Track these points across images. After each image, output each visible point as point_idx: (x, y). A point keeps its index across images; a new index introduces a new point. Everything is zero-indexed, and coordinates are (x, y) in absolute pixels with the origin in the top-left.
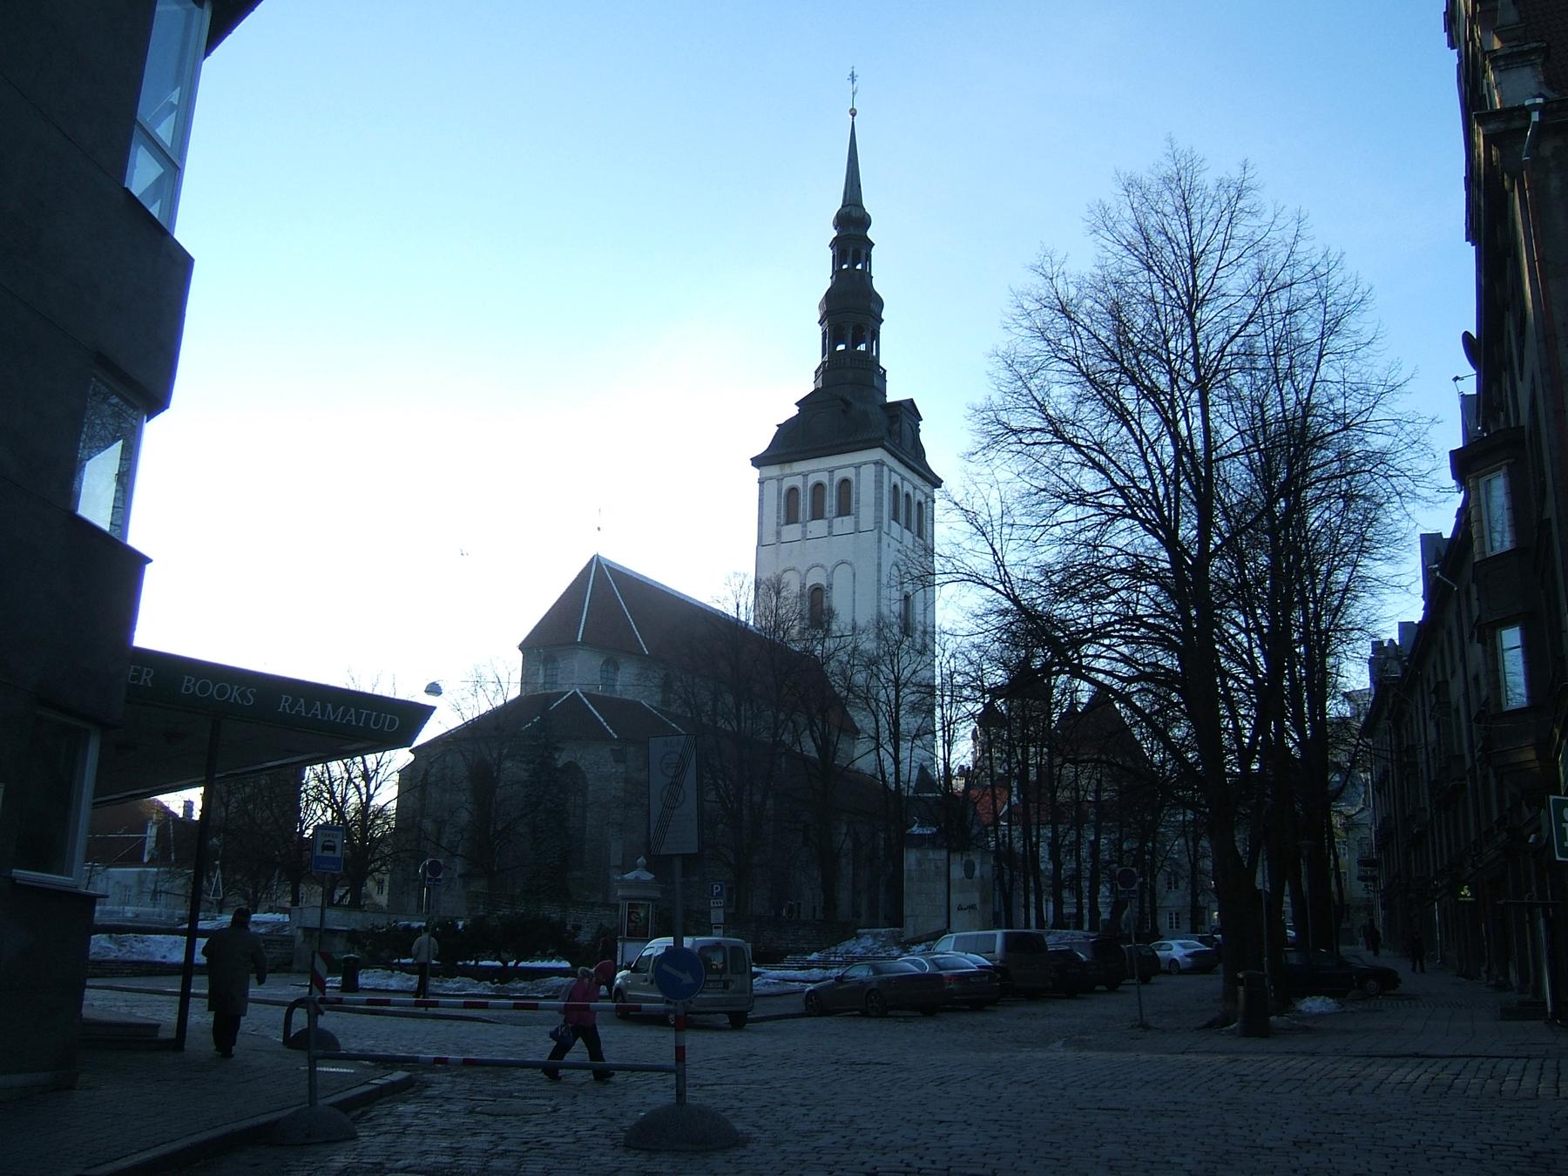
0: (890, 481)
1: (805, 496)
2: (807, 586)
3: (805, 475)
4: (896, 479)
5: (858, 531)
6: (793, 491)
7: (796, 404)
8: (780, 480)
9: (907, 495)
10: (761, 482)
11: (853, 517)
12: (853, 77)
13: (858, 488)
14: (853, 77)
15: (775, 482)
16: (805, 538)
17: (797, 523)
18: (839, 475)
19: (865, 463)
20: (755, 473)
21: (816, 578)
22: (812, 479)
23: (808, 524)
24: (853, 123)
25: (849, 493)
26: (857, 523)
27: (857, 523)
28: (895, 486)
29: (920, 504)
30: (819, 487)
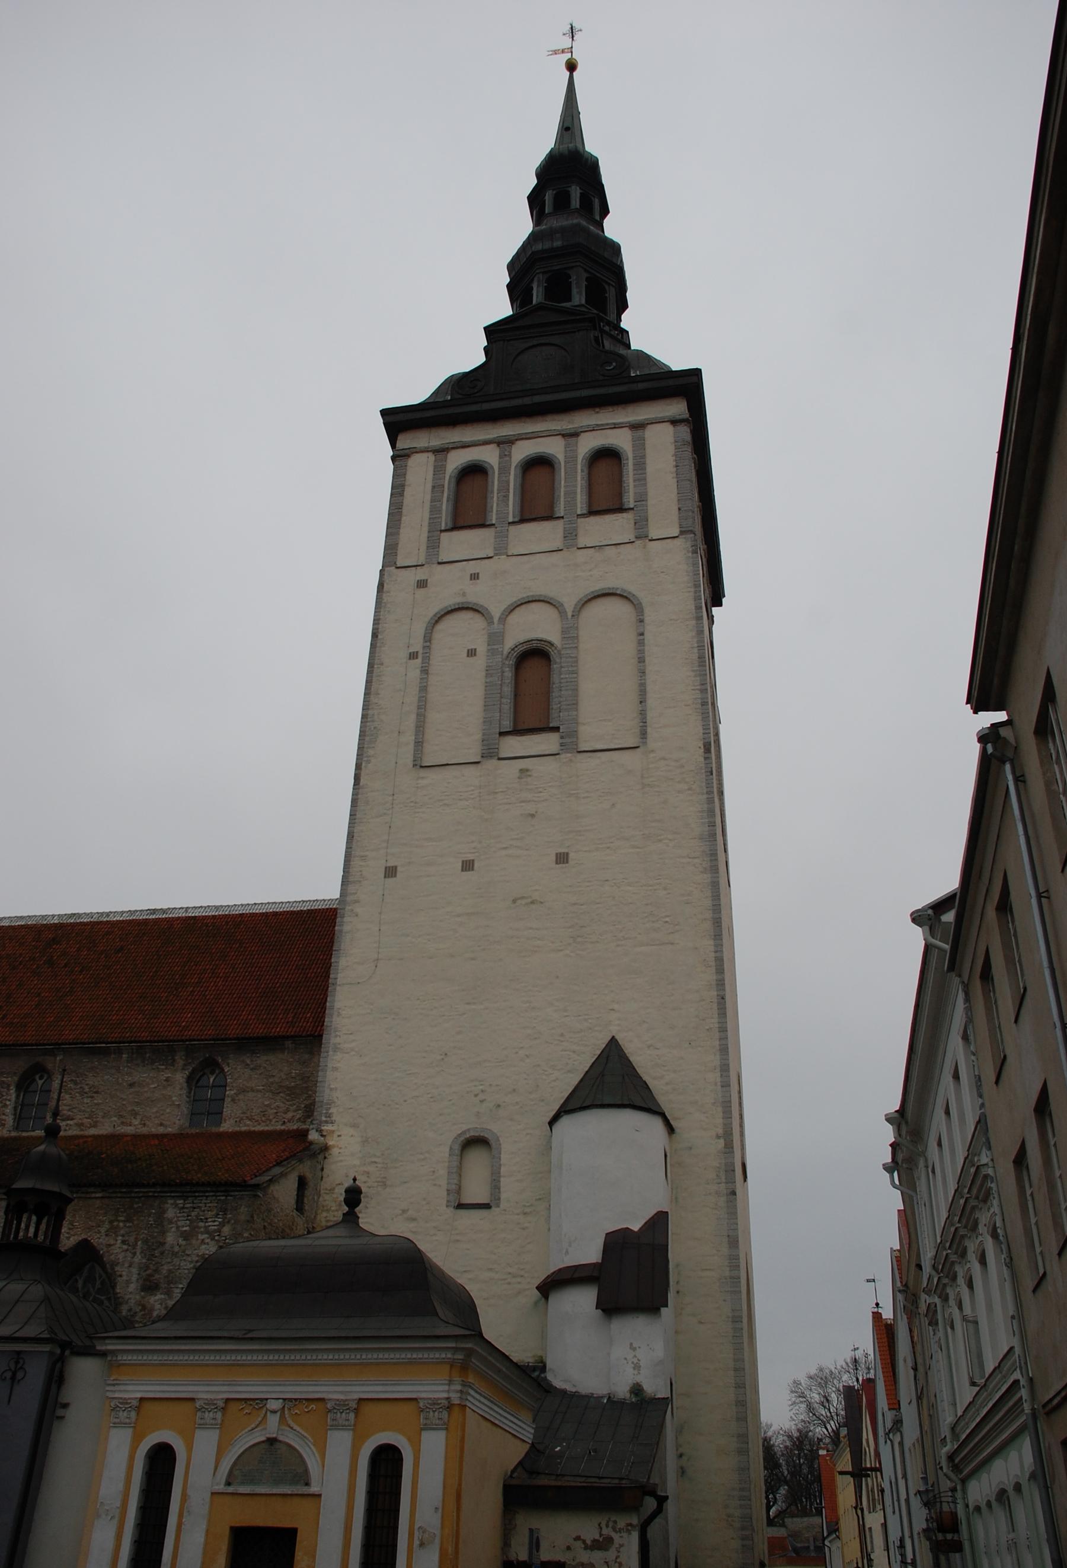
2: (509, 643)
5: (642, 534)
6: (474, 471)
8: (441, 451)
15: (431, 457)
17: (483, 526)
23: (512, 528)
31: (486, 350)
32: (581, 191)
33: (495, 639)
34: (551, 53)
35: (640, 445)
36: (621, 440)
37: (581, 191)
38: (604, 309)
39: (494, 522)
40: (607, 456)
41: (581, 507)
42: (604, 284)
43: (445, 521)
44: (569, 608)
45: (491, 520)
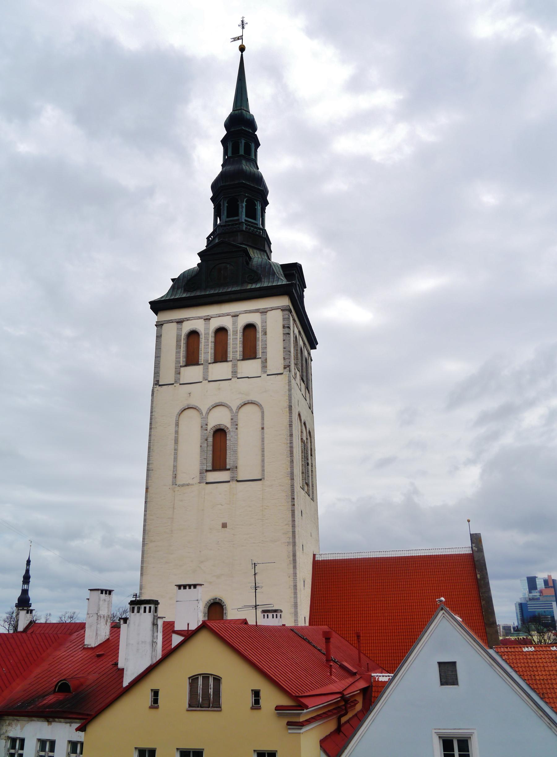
1: (207, 339)
2: (209, 427)
3: (207, 319)
8: (180, 322)
10: (159, 325)
15: (175, 324)
16: (205, 379)
19: (273, 309)
22: (215, 324)
23: (211, 366)
24: (242, 55)
25: (255, 339)
26: (264, 366)
27: (264, 366)
28: (296, 337)
30: (221, 332)
31: (198, 265)
32: (245, 141)
34: (232, 40)
35: (264, 322)
36: (255, 319)
37: (245, 141)
38: (255, 218)
39: (202, 363)
40: (250, 328)
41: (239, 355)
43: (182, 361)
44: (234, 409)
45: (201, 361)
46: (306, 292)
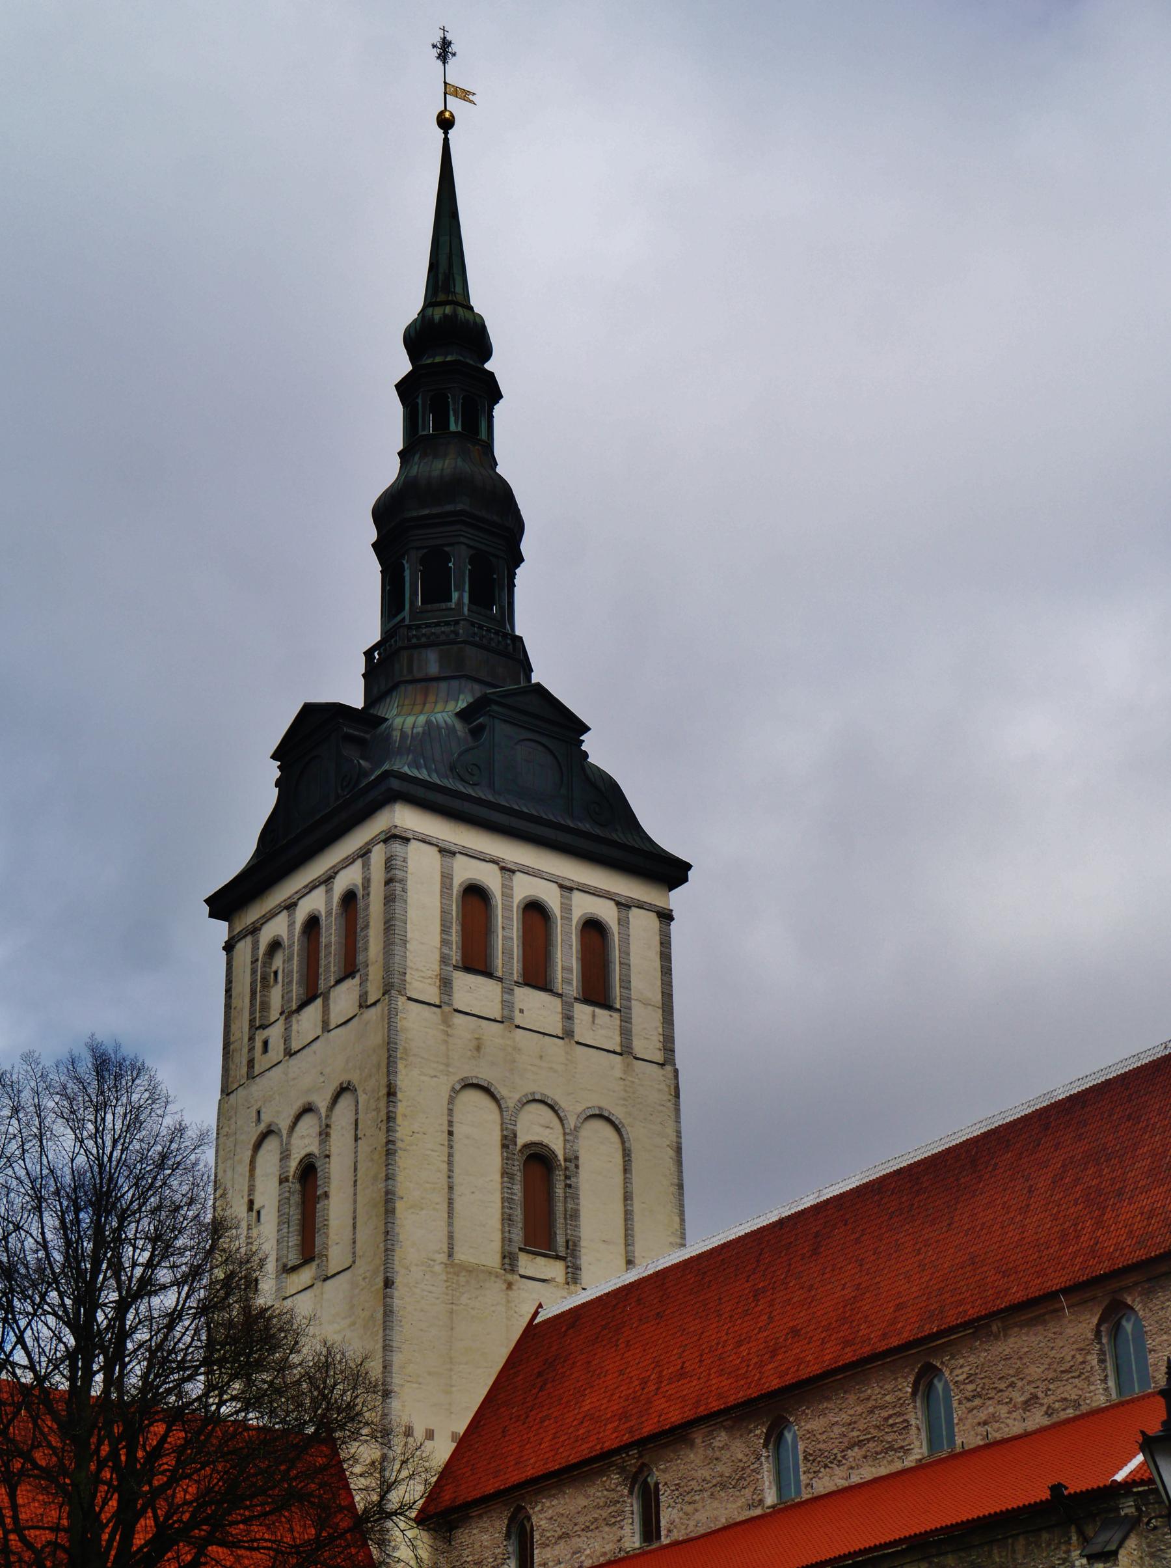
0: (446, 878)
4: (466, 871)
7: (275, 757)
8: (254, 930)
9: (535, 909)
10: (229, 947)
11: (358, 976)
12: (444, 50)
13: (367, 906)
14: (444, 50)
18: (341, 884)
20: (221, 929)
21: (304, 1142)
22: (301, 914)
24: (446, 141)
29: (593, 928)
33: (285, 1156)
35: (367, 882)
42: (446, 549)
46: (589, 743)
